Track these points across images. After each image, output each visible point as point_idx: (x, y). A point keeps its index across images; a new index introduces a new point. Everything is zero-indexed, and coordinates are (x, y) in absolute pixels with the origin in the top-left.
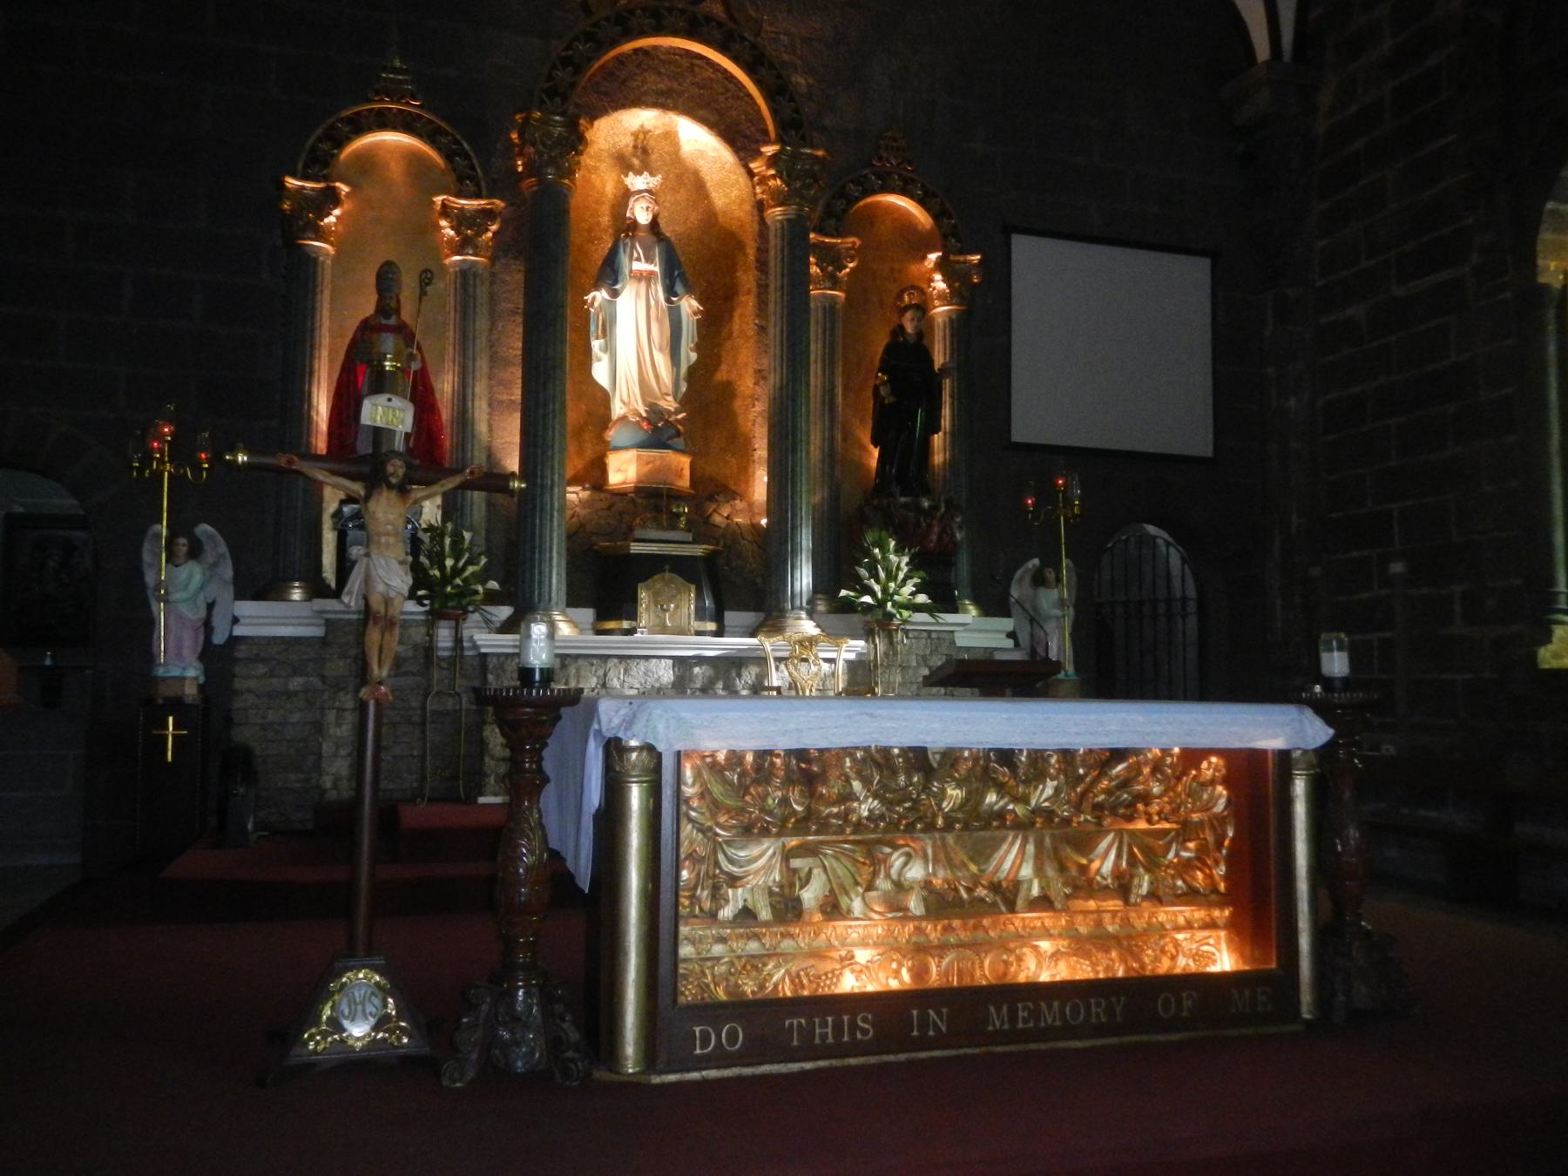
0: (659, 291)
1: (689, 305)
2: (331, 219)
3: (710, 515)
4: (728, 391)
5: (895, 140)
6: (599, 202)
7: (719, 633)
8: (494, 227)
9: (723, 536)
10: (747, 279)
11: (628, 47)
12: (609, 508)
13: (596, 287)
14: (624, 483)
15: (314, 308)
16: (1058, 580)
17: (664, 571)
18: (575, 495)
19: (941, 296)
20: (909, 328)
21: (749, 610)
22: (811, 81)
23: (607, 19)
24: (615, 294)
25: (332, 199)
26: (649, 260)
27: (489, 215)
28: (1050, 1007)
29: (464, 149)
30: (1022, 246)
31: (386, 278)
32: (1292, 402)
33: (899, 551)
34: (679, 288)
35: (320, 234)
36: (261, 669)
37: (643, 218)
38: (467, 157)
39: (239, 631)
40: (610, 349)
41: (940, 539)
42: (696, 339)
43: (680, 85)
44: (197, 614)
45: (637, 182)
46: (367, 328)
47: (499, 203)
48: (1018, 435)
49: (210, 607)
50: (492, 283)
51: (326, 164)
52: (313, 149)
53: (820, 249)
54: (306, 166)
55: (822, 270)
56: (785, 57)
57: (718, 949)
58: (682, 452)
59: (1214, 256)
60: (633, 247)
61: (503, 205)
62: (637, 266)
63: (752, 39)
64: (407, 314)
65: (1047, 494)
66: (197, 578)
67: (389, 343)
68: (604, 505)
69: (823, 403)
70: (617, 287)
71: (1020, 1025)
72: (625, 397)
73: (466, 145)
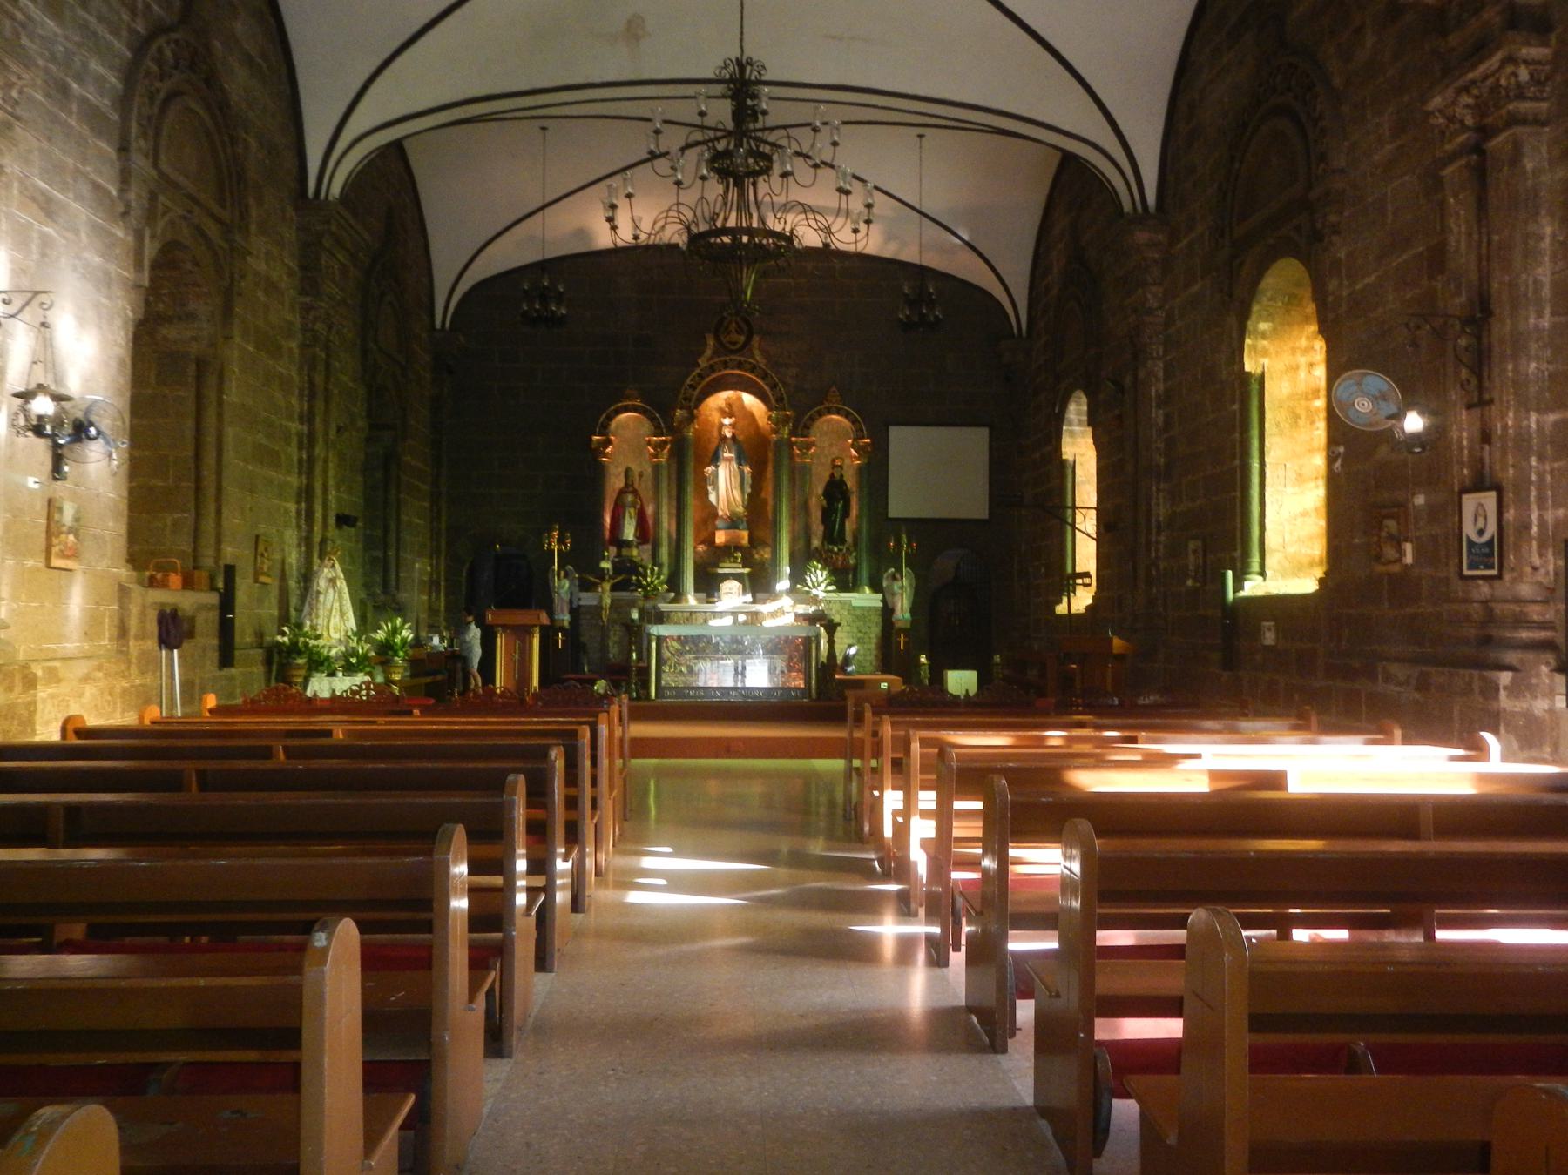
1: (747, 469)
2: (608, 450)
4: (765, 502)
6: (713, 427)
7: (754, 602)
8: (669, 446)
10: (770, 455)
11: (714, 376)
16: (902, 577)
18: (701, 548)
19: (855, 457)
24: (717, 467)
25: (609, 442)
26: (730, 452)
27: (665, 442)
30: (897, 434)
31: (628, 472)
33: (822, 569)
36: (588, 617)
37: (729, 435)
39: (582, 603)
40: (716, 489)
41: (842, 563)
42: (750, 482)
44: (566, 597)
45: (727, 421)
46: (622, 492)
47: (669, 438)
48: (891, 515)
49: (571, 595)
58: (743, 529)
62: (725, 455)
64: (636, 485)
65: (898, 543)
66: (567, 585)
67: (630, 498)
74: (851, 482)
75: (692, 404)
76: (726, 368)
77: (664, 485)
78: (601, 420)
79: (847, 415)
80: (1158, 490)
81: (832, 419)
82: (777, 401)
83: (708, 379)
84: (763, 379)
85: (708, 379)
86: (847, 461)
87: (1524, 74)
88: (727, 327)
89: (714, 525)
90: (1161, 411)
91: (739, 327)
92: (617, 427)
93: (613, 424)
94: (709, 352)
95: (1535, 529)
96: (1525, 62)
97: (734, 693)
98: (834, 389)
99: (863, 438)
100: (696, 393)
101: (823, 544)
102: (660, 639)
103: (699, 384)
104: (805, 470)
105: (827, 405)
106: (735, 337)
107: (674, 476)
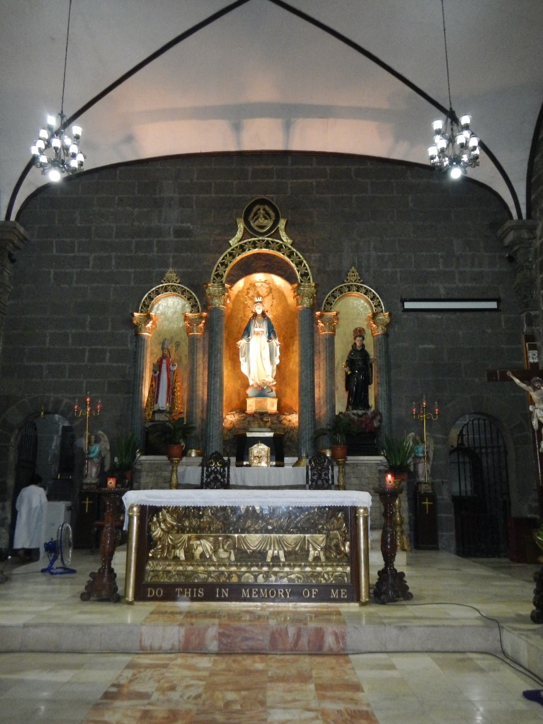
0: (264, 338)
1: (276, 342)
2: (149, 325)
3: (282, 421)
5: (353, 272)
8: (204, 321)
9: (287, 428)
11: (244, 255)
12: (244, 420)
13: (241, 338)
14: (251, 410)
15: (144, 356)
17: (258, 443)
20: (358, 344)
21: (294, 456)
22: (320, 254)
23: (237, 247)
24: (249, 340)
28: (264, 591)
29: (193, 296)
34: (272, 336)
37: (259, 312)
38: (195, 299)
40: (247, 360)
42: (278, 354)
43: (270, 263)
50: (203, 342)
52: (144, 302)
54: (142, 308)
55: (325, 325)
56: (310, 247)
57: (170, 568)
58: (273, 397)
60: (255, 323)
61: (206, 314)
62: (257, 330)
63: (290, 246)
68: (243, 418)
69: (326, 375)
70: (250, 338)
71: (253, 596)
72: (253, 379)
73: (193, 294)
75: (224, 279)
76: (255, 247)
77: (200, 355)
78: (144, 299)
83: (238, 258)
84: (289, 257)
85: (238, 258)
88: (256, 214)
89: (247, 395)
91: (267, 213)
94: (239, 235)
98: (353, 268)
100: (228, 269)
101: (347, 408)
103: (230, 262)
106: (261, 221)
107: (207, 349)
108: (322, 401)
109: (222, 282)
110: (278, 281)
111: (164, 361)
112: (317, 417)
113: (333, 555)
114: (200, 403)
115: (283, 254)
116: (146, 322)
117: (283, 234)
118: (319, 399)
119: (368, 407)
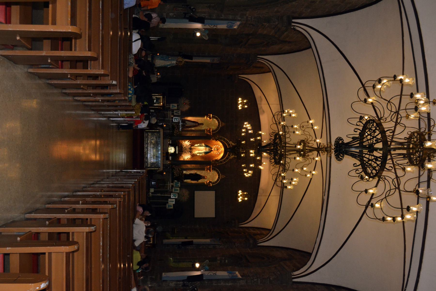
0: (204, 151)
1: (203, 154)
2: (208, 118)
13: (205, 145)
19: (207, 182)
20: (202, 177)
24: (204, 146)
25: (210, 118)
26: (208, 150)
27: (210, 133)
32: (198, 226)
35: (207, 117)
37: (212, 149)
40: (198, 146)
42: (200, 155)
51: (214, 118)
53: (210, 167)
59: (215, 218)
62: (207, 149)
74: (200, 181)
79: (218, 180)
80: (194, 247)
81: (217, 176)
82: (221, 161)
84: (226, 158)
86: (206, 180)
87: (255, 280)
90: (212, 247)
92: (214, 120)
93: (215, 120)
95: (178, 283)
96: (258, 280)
97: (146, 150)
98: (225, 176)
99: (212, 184)
100: (223, 141)
102: (159, 132)
104: (203, 169)
105: (220, 175)
108: (186, 167)
109: (219, 139)
110: (222, 155)
111: (197, 124)
112: (182, 165)
113: (152, 164)
114: (186, 133)
115: (227, 156)
116: (209, 118)
117: (233, 156)
118: (187, 166)
119: (185, 180)
